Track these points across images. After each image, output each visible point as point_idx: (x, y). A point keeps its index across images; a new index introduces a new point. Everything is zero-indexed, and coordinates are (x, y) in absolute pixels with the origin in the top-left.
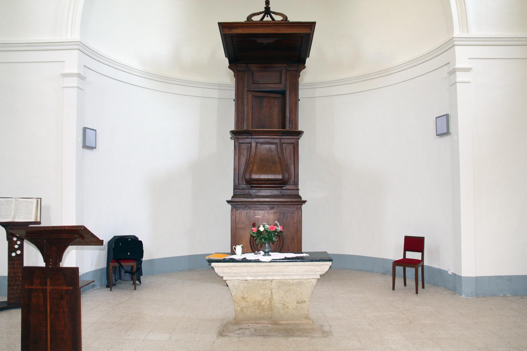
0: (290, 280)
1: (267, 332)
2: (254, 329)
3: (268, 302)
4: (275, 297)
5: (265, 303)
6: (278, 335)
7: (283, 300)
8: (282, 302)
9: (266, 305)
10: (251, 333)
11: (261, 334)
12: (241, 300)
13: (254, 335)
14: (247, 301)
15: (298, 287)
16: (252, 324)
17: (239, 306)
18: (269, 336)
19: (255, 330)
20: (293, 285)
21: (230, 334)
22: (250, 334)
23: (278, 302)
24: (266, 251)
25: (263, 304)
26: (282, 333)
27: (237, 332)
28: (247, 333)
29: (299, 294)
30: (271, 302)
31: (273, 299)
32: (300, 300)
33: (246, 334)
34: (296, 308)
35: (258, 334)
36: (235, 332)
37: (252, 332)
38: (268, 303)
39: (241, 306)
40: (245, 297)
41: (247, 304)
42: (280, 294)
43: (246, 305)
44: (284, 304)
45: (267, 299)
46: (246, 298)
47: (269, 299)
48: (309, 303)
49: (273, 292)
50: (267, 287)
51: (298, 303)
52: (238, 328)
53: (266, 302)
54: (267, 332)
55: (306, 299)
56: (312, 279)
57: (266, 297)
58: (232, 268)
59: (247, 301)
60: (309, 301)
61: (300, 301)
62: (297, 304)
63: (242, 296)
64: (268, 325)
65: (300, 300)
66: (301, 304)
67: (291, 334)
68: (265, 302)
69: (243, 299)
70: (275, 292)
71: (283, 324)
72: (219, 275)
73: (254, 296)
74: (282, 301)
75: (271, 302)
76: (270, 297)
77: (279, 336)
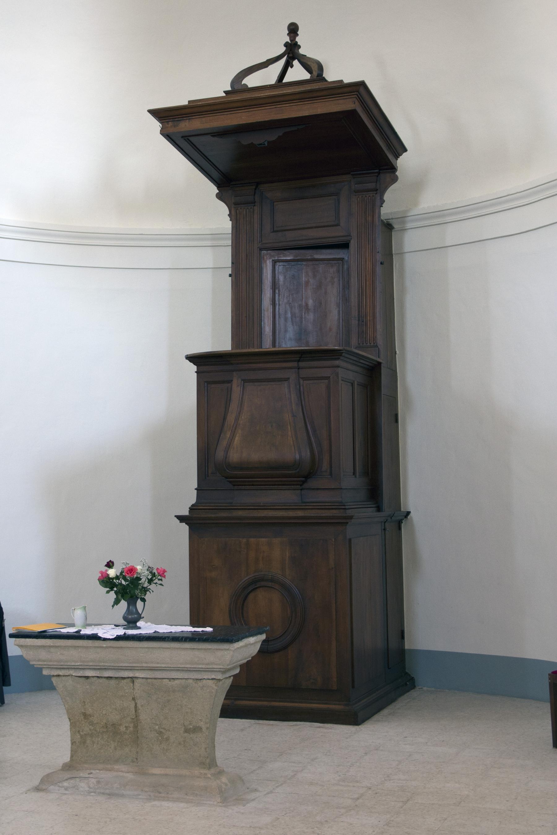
0: (164, 680)
1: (119, 787)
2: (96, 780)
3: (132, 725)
4: (144, 716)
5: (125, 729)
6: (139, 795)
7: (158, 723)
8: (157, 727)
9: (128, 732)
10: (89, 787)
11: (107, 791)
12: (82, 721)
13: (95, 792)
14: (92, 723)
15: (184, 696)
16: (99, 770)
17: (79, 731)
18: (123, 796)
19: (98, 782)
20: (174, 691)
21: (52, 787)
22: (87, 789)
23: (150, 728)
24: (130, 618)
25: (122, 729)
26: (146, 791)
27: (65, 784)
28: (82, 787)
29: (187, 713)
30: (136, 727)
31: (139, 720)
32: (190, 724)
33: (82, 789)
34: (182, 743)
35: (102, 791)
36: (60, 785)
37: (92, 786)
38: (131, 729)
39: (82, 732)
40: (88, 713)
41: (92, 728)
42: (152, 710)
43: (90, 729)
44: (161, 732)
45: (129, 719)
46: (90, 716)
47: (133, 719)
48: (207, 733)
49: (139, 705)
50: (127, 693)
51: (187, 731)
52: (69, 776)
53: (127, 725)
54: (119, 787)
55: (202, 724)
56: (208, 681)
57: (126, 715)
58: (52, 650)
59: (92, 723)
60: (207, 728)
61: (190, 728)
62: (186, 734)
63: (83, 711)
64: (127, 775)
65: (190, 724)
66: (192, 735)
67: (163, 795)
68: (126, 727)
69: (85, 718)
70: (142, 706)
71: (155, 775)
72: (33, 665)
73: (104, 713)
74: (157, 725)
75: (136, 727)
76: (135, 716)
77: (140, 797)
